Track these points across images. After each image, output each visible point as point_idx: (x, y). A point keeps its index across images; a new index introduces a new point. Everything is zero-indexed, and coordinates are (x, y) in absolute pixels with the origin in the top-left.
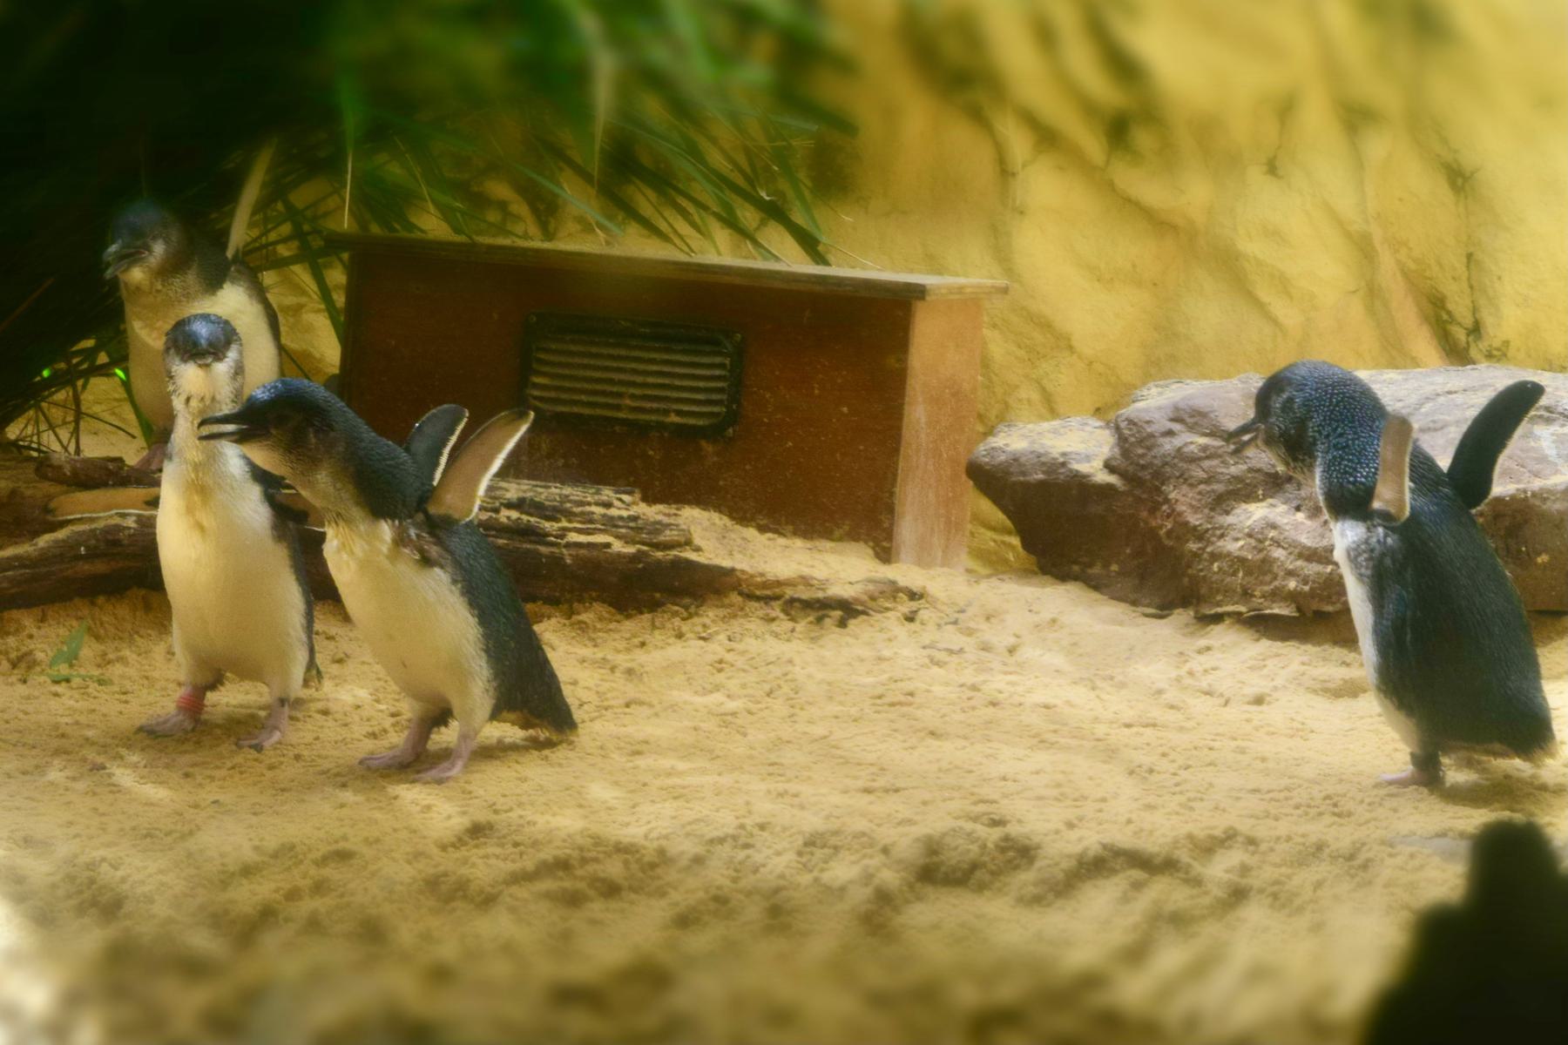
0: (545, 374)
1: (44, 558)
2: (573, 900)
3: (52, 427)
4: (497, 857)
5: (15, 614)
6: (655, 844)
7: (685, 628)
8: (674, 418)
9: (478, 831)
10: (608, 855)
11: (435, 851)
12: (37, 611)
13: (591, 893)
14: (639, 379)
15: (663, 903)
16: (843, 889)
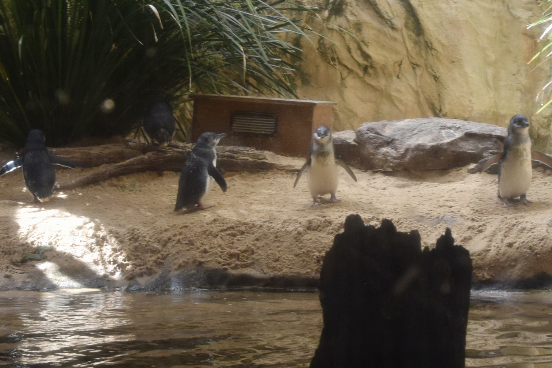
0: (236, 124)
1: (128, 165)
2: (234, 235)
4: (219, 226)
6: (252, 223)
7: (265, 176)
8: (264, 133)
9: (215, 221)
10: (242, 225)
11: (206, 225)
13: (238, 234)
14: (256, 124)
15: (254, 235)
16: (291, 232)
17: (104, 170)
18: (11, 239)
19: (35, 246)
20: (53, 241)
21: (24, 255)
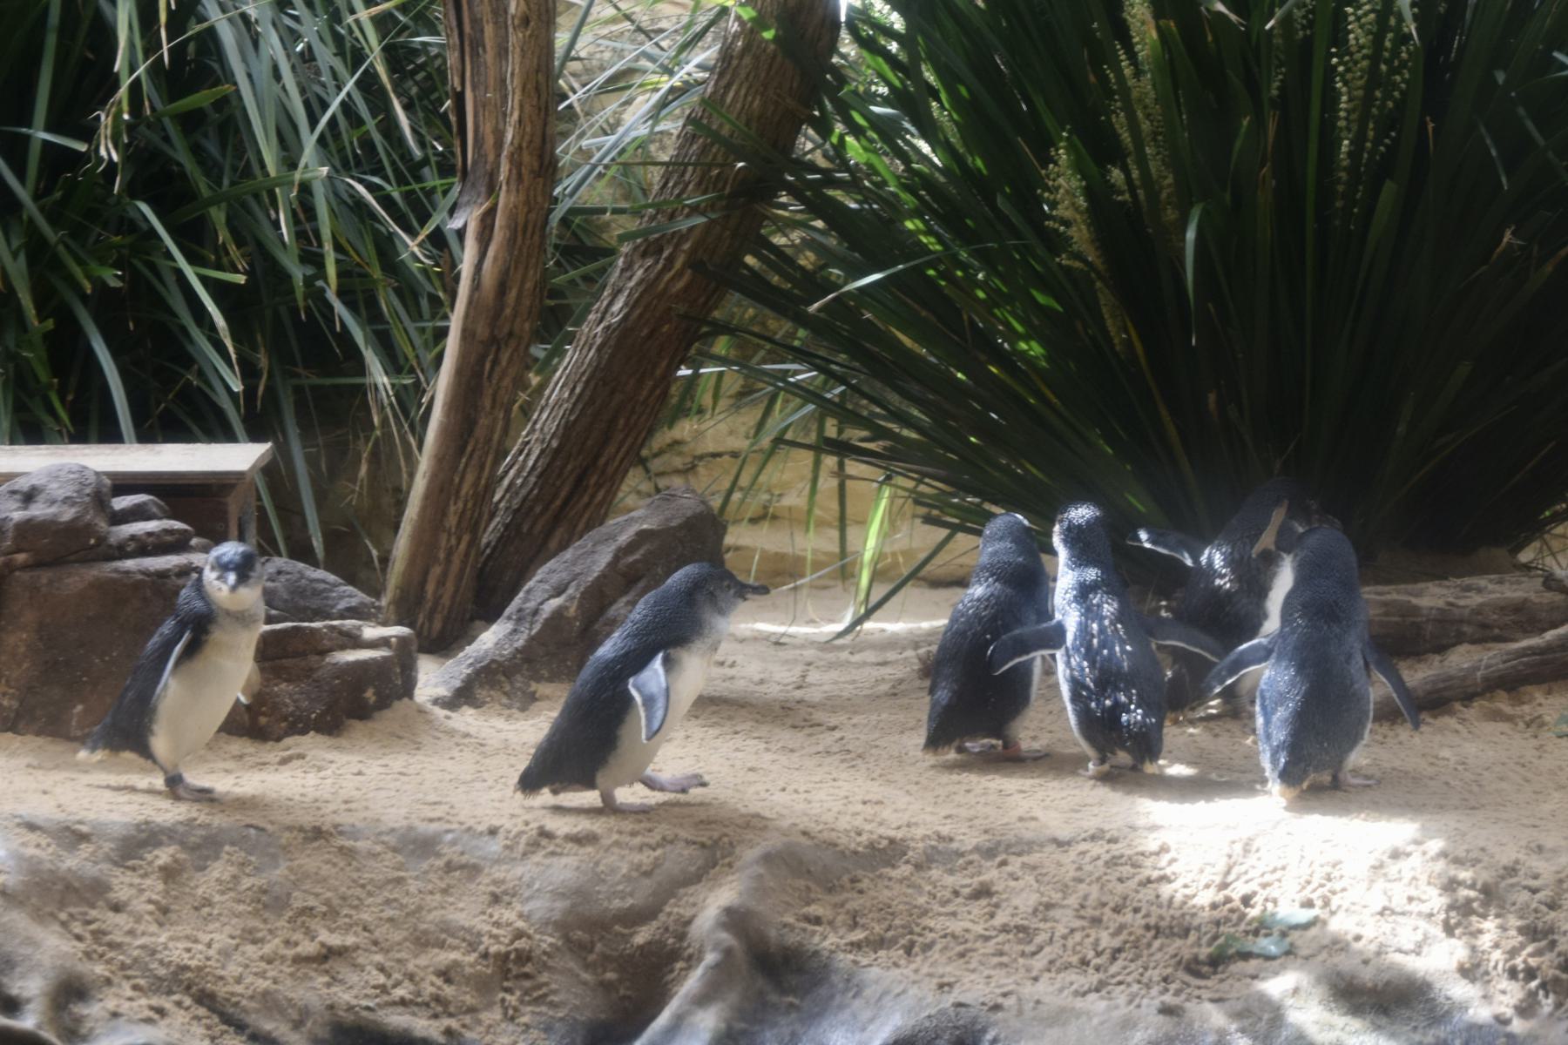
1: (1548, 649)
3: (1553, 554)
5: (1529, 688)
12: (1545, 686)
17: (1466, 666)
18: (1174, 886)
19: (1253, 913)
20: (1314, 896)
21: (1221, 941)
